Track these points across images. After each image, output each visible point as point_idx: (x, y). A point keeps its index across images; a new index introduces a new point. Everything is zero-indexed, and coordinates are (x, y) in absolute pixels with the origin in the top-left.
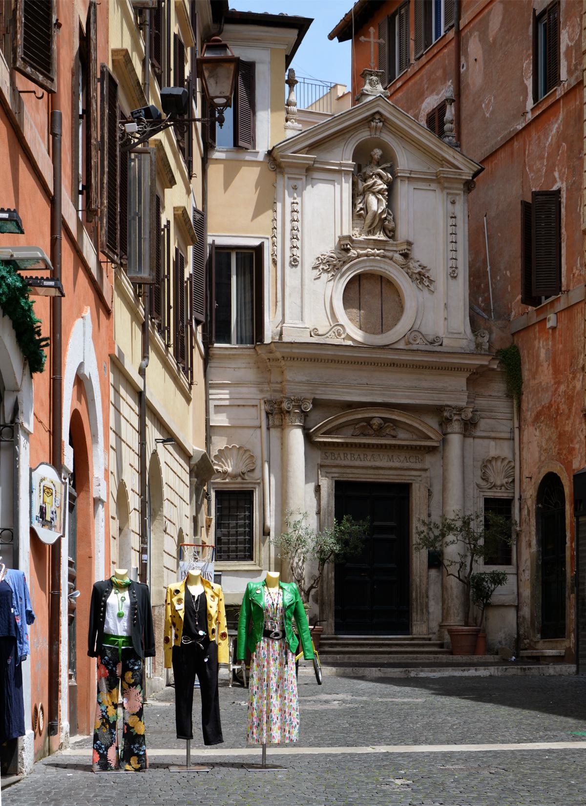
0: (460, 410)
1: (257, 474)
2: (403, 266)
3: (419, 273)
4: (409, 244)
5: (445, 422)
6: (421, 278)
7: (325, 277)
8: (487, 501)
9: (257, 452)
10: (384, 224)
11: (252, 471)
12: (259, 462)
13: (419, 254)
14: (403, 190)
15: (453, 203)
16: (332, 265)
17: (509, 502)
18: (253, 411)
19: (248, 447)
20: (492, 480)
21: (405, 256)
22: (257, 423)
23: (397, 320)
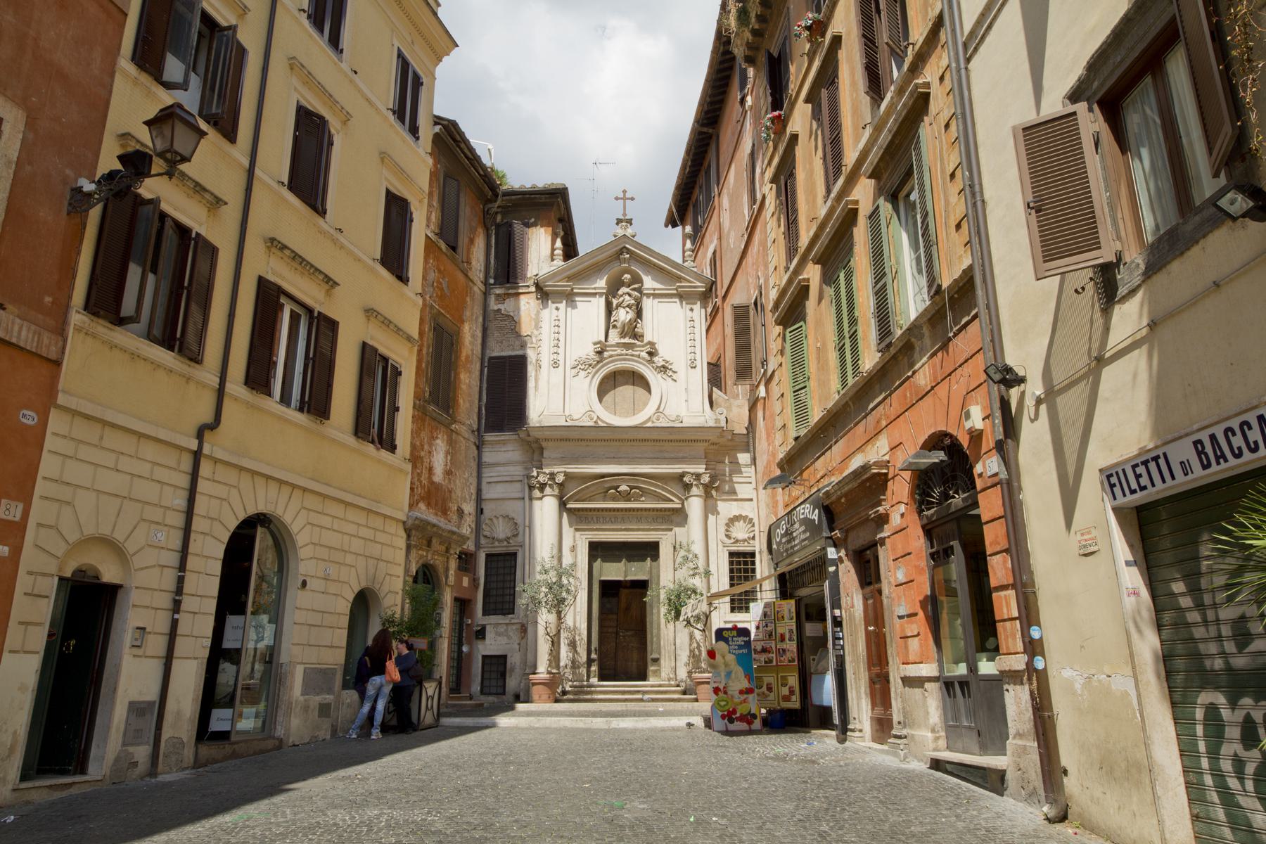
0: (698, 476)
1: (520, 538)
2: (651, 362)
3: (663, 366)
4: (652, 344)
5: (687, 487)
6: (664, 369)
7: (582, 373)
8: (731, 554)
9: (519, 521)
10: (632, 331)
11: (516, 535)
12: (521, 529)
13: (664, 353)
14: (648, 304)
15: (692, 310)
16: (583, 365)
17: (753, 555)
18: (518, 485)
19: (512, 515)
20: (734, 535)
21: (651, 354)
22: (520, 495)
23: (646, 404)
